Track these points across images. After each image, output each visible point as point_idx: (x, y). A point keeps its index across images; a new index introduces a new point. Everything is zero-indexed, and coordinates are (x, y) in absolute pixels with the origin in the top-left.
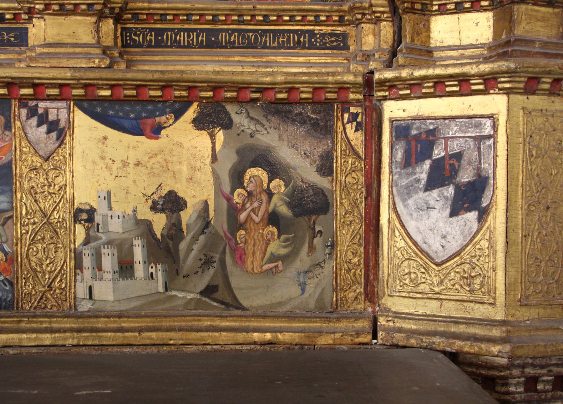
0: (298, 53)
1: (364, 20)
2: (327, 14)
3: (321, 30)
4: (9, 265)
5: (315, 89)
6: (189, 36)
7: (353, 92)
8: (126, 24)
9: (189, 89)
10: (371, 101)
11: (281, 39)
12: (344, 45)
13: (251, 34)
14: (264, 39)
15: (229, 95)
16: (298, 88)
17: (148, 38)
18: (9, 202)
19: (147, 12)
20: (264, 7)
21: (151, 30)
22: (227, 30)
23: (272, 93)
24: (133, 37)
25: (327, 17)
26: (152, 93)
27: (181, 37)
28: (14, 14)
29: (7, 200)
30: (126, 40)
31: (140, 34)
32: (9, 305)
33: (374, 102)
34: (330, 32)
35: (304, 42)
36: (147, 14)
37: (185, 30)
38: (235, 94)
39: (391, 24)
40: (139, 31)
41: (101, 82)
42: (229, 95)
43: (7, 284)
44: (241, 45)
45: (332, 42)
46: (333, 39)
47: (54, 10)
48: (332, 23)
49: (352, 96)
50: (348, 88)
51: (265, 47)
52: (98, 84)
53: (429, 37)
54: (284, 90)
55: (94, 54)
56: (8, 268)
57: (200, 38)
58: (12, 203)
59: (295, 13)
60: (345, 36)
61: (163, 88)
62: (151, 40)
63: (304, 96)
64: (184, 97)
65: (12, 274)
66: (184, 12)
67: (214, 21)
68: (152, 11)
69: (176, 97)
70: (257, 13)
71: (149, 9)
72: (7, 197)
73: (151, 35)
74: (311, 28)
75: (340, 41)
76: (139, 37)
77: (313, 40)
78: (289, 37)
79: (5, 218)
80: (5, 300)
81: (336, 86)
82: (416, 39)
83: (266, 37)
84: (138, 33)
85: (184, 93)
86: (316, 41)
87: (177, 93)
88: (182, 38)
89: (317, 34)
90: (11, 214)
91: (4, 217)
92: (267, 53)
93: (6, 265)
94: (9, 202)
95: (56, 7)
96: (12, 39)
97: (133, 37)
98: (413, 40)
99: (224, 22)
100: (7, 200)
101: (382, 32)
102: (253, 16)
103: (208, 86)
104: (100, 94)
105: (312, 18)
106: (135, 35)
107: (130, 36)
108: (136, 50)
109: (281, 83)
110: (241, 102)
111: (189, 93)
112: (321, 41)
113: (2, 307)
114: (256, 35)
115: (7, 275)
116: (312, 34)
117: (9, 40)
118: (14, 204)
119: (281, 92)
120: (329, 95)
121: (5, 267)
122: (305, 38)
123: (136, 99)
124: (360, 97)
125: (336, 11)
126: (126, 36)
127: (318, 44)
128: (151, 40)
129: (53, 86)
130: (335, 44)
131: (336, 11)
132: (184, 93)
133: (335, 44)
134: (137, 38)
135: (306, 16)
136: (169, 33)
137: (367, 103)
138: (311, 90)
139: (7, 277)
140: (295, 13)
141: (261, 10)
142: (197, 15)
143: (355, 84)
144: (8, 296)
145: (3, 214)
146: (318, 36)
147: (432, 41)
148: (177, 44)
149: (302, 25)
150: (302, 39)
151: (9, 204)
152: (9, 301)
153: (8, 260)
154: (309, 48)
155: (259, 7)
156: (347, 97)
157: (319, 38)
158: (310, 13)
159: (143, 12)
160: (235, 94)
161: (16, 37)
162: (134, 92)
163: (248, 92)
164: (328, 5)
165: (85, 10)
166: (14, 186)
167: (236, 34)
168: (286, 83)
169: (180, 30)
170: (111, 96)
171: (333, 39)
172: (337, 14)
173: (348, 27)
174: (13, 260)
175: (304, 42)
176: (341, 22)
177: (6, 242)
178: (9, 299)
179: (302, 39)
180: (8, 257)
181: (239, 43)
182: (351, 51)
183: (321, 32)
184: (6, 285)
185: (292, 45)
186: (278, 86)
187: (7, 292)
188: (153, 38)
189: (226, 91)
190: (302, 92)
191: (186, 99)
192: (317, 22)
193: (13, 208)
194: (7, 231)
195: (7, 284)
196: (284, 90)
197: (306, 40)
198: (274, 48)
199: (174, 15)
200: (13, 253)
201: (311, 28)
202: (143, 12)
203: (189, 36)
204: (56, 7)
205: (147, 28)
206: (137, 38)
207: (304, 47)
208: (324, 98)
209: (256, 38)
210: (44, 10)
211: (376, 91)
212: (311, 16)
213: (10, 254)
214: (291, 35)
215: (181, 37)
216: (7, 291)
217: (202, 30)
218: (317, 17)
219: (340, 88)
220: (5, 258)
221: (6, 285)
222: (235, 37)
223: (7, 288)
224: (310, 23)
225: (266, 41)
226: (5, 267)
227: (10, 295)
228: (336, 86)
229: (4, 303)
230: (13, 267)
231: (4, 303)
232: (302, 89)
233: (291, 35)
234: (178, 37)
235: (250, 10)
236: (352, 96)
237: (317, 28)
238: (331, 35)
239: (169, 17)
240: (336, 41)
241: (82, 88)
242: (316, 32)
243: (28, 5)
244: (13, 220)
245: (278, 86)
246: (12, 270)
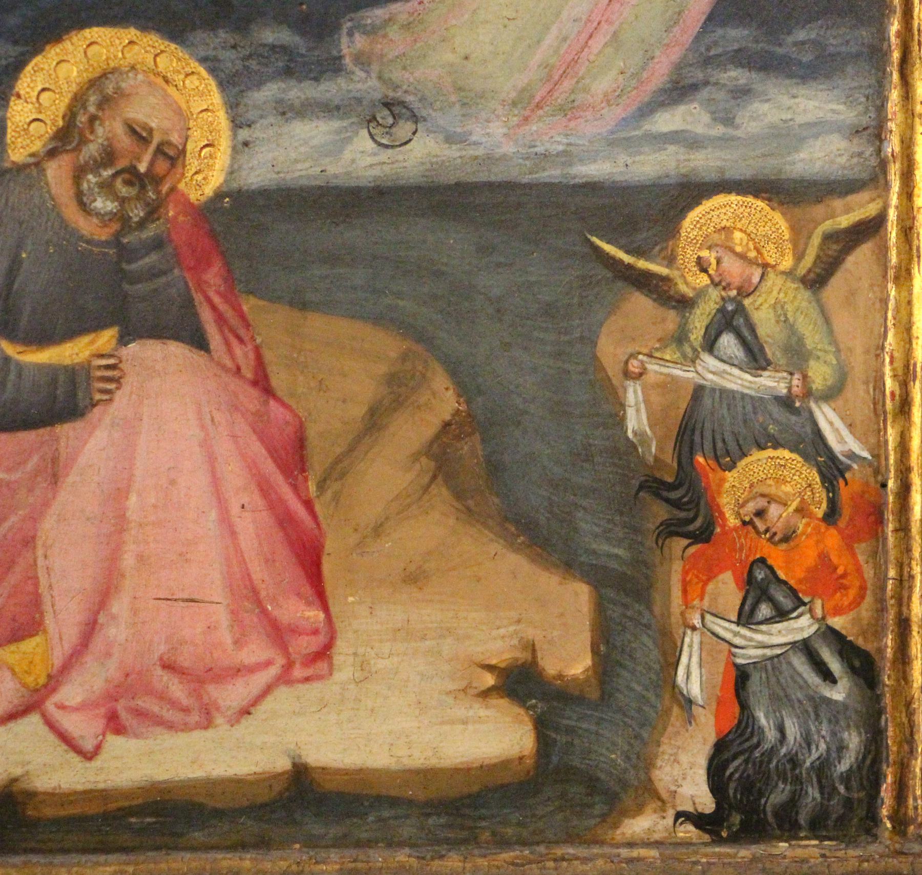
4: (849, 541)
18: (857, 132)
29: (848, 115)
32: (848, 803)
43: (835, 666)
56: (842, 564)
58: (878, 134)
65: (869, 599)
72: (849, 100)
79: (828, 238)
80: (822, 768)
90: (871, 210)
91: (827, 226)
93: (832, 539)
94: (857, 132)
100: (848, 115)
113: (803, 819)
115: (838, 611)
118: (893, 145)
121: (823, 557)
139: (837, 622)
144: (841, 748)
145: (819, 210)
151: (858, 144)
152: (846, 778)
153: (846, 512)
166: (895, 27)
174: (877, 515)
177: (830, 395)
178: (843, 767)
180: (845, 493)
184: (828, 676)
187: (834, 720)
193: (883, 165)
194: (842, 321)
195: (835, 666)
200: (877, 469)
213: (856, 474)
216: (836, 712)
220: (821, 495)
221: (828, 676)
223: (838, 694)
226: (823, 557)
227: (854, 740)
229: (813, 793)
230: (877, 554)
231: (813, 793)
244: (883, 250)
246: (869, 573)
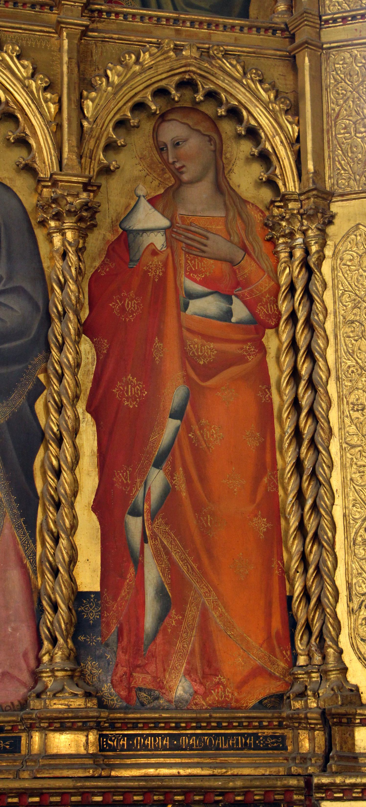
0: (245, 754)
1: (300, 727)
2: (269, 720)
3: (264, 733)
5: (266, 792)
6: (155, 740)
7: (296, 794)
8: (103, 731)
9: (165, 794)
10: (310, 800)
11: (231, 742)
12: (283, 745)
13: (206, 738)
14: (217, 742)
15: (197, 798)
16: (253, 791)
17: (121, 743)
19: (122, 721)
20: (218, 715)
21: (124, 735)
22: (186, 735)
23: (231, 796)
24: (109, 742)
25: (269, 722)
26: (136, 798)
27: (148, 742)
28: (12, 726)
30: (103, 745)
31: (114, 740)
33: (313, 801)
34: (271, 734)
35: (250, 744)
36: (122, 723)
37: (151, 735)
38: (202, 797)
39: (323, 733)
40: (114, 736)
41: (96, 790)
42: (197, 798)
44: (198, 748)
45: (273, 743)
46: (273, 740)
47: (55, 727)
48: (273, 727)
49: (295, 797)
50: (293, 790)
51: (218, 749)
52: (94, 792)
53: (354, 744)
54: (242, 794)
55: (87, 764)
57: (165, 742)
59: (243, 720)
60: (283, 738)
61: (144, 794)
62: (123, 744)
63: (257, 798)
64: (161, 800)
66: (153, 721)
67: (177, 727)
68: (126, 721)
69: (155, 801)
70: (212, 720)
71: (124, 719)
73: (124, 740)
74: (255, 731)
75: (280, 742)
76: (113, 742)
77: (257, 742)
78: (237, 740)
81: (283, 789)
82: (344, 747)
83: (219, 740)
84: (113, 738)
85: (161, 798)
86: (260, 742)
87: (156, 798)
88: (149, 742)
89: (260, 736)
92: (220, 754)
95: (58, 725)
96: (8, 747)
97: (109, 742)
98: (341, 748)
99: (185, 728)
101: (316, 739)
102: (209, 723)
103: (182, 791)
104: (94, 800)
105: (257, 724)
106: (111, 740)
107: (106, 741)
108: (111, 753)
109: (240, 788)
110: (206, 804)
111: (165, 798)
112: (264, 742)
114: (210, 739)
116: (256, 736)
117: (4, 748)
119: (239, 795)
120: (277, 797)
122: (250, 740)
123: (122, 803)
124: (302, 798)
125: (276, 718)
126: (103, 741)
127: (261, 746)
128: (123, 744)
129: (57, 794)
130: (275, 745)
131: (276, 718)
132: (161, 798)
133: (275, 745)
134: (112, 743)
135: (252, 722)
136: (139, 738)
137: (307, 803)
138: (263, 793)
140: (243, 720)
141: (216, 718)
142: (163, 723)
143: (298, 787)
146: (261, 738)
147: (357, 748)
148: (145, 747)
149: (248, 729)
150: (248, 741)
154: (254, 749)
155: (214, 715)
156: (292, 798)
157: (262, 740)
158: (255, 720)
159: (119, 721)
160: (202, 797)
161: (11, 745)
162: (121, 798)
163: (212, 795)
164: (271, 712)
165: (80, 726)
167: (194, 738)
168: (244, 788)
169: (148, 735)
170: (102, 801)
171: (273, 740)
172: (277, 720)
173: (286, 730)
175: (250, 744)
176: (280, 726)
179: (248, 741)
181: (196, 746)
182: (289, 751)
183: (264, 735)
185: (240, 746)
186: (237, 790)
188: (125, 743)
189: (195, 795)
190: (256, 795)
191: (162, 802)
192: (261, 727)
196: (242, 794)
197: (252, 742)
198: (226, 749)
199: (144, 723)
201: (255, 731)
202: (119, 721)
203: (155, 740)
204: (58, 725)
205: (120, 734)
206: (112, 743)
207: (250, 748)
208: (272, 798)
209: (211, 741)
210: (48, 727)
211: (315, 793)
212: (256, 722)
214: (240, 738)
215: (148, 742)
217: (166, 735)
218: (260, 723)
219: (286, 791)
222: (193, 741)
224: (255, 728)
225: (219, 743)
228: (283, 789)
232: (256, 792)
233: (240, 738)
234: (146, 742)
235: (207, 718)
236: (295, 797)
237: (260, 731)
238: (272, 737)
239: (140, 725)
240: (277, 742)
241: (80, 795)
242: (260, 734)
243: (31, 721)
245: (237, 790)
